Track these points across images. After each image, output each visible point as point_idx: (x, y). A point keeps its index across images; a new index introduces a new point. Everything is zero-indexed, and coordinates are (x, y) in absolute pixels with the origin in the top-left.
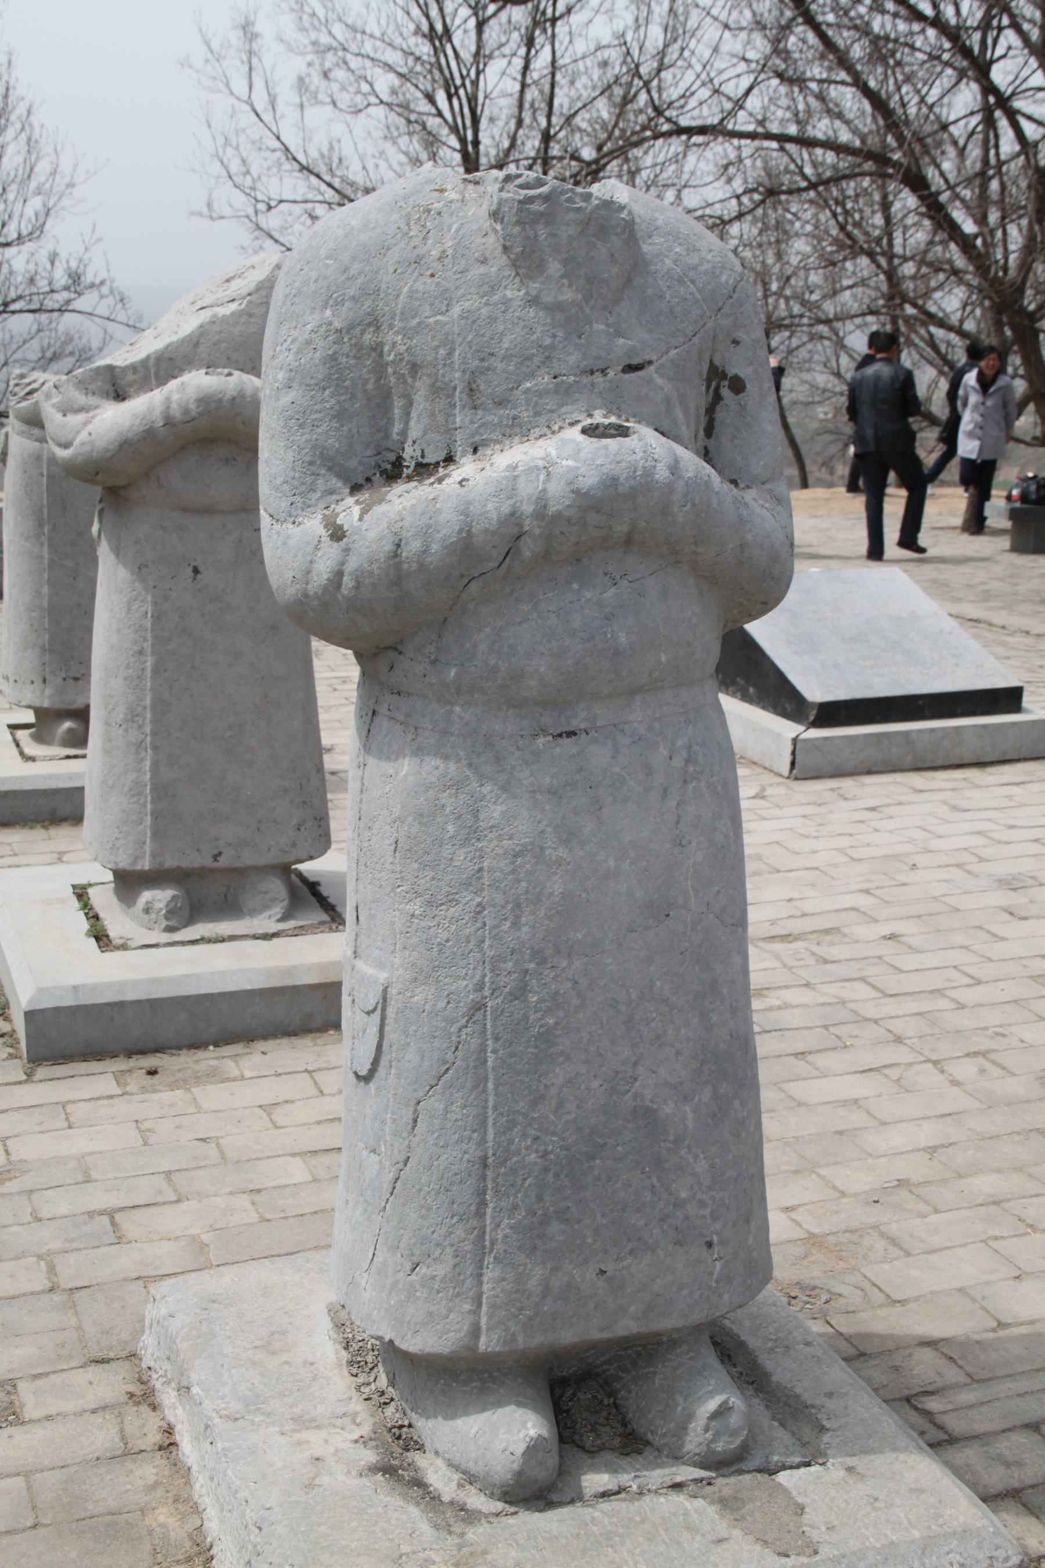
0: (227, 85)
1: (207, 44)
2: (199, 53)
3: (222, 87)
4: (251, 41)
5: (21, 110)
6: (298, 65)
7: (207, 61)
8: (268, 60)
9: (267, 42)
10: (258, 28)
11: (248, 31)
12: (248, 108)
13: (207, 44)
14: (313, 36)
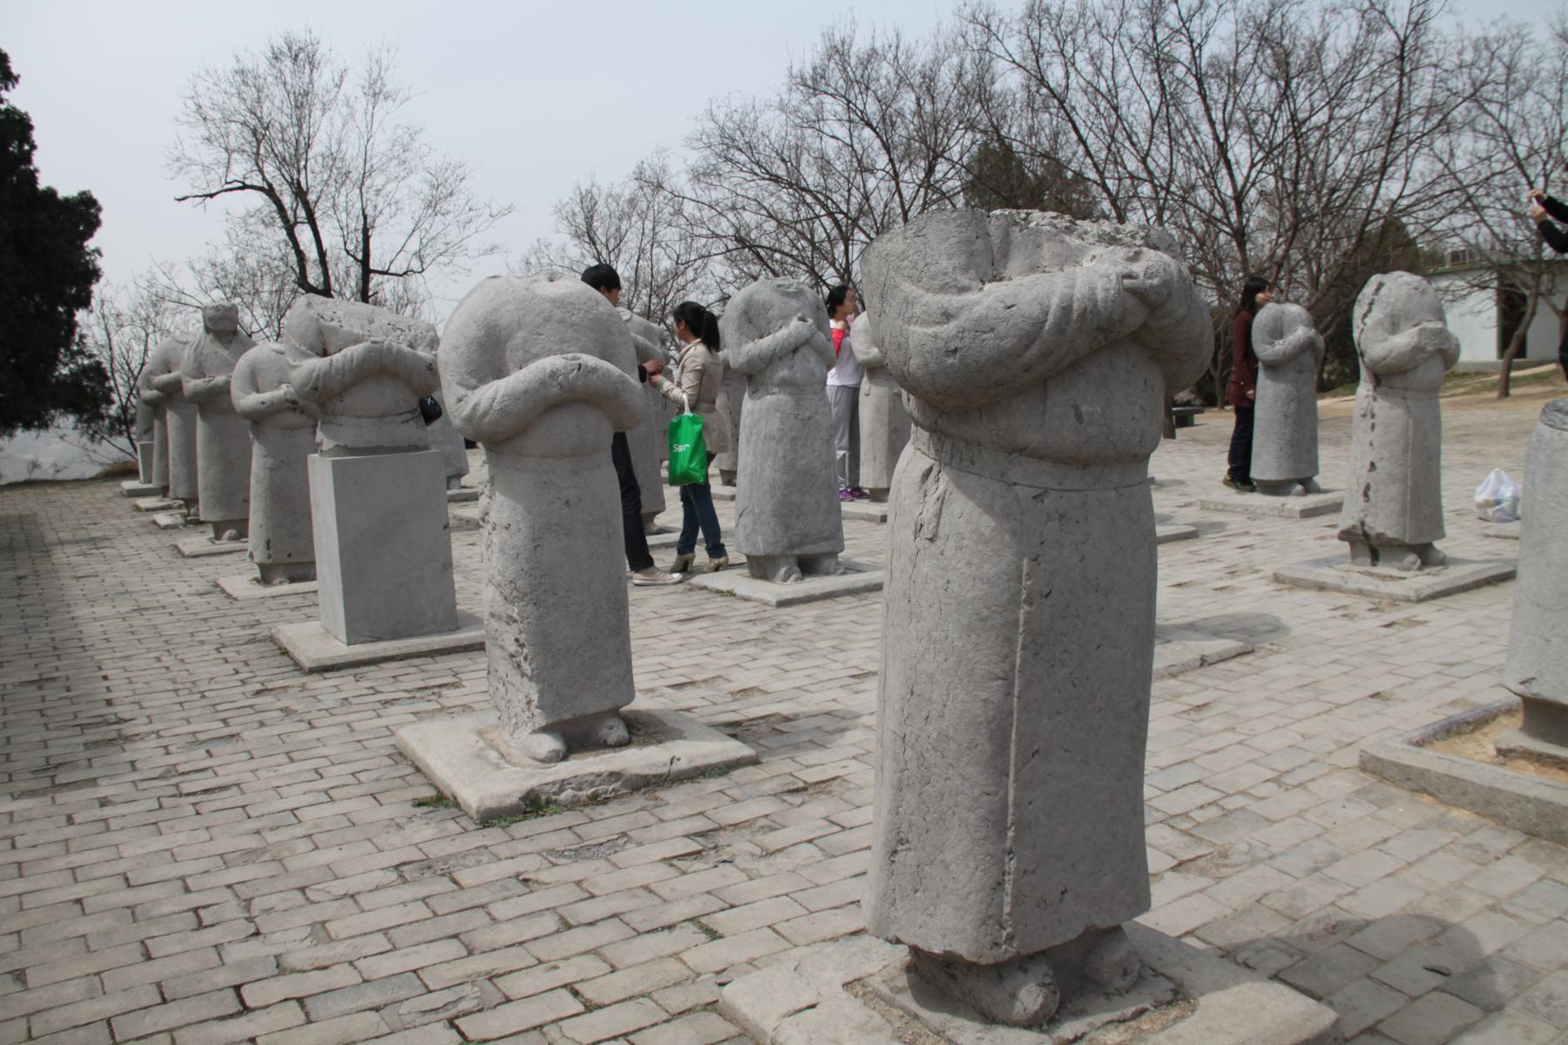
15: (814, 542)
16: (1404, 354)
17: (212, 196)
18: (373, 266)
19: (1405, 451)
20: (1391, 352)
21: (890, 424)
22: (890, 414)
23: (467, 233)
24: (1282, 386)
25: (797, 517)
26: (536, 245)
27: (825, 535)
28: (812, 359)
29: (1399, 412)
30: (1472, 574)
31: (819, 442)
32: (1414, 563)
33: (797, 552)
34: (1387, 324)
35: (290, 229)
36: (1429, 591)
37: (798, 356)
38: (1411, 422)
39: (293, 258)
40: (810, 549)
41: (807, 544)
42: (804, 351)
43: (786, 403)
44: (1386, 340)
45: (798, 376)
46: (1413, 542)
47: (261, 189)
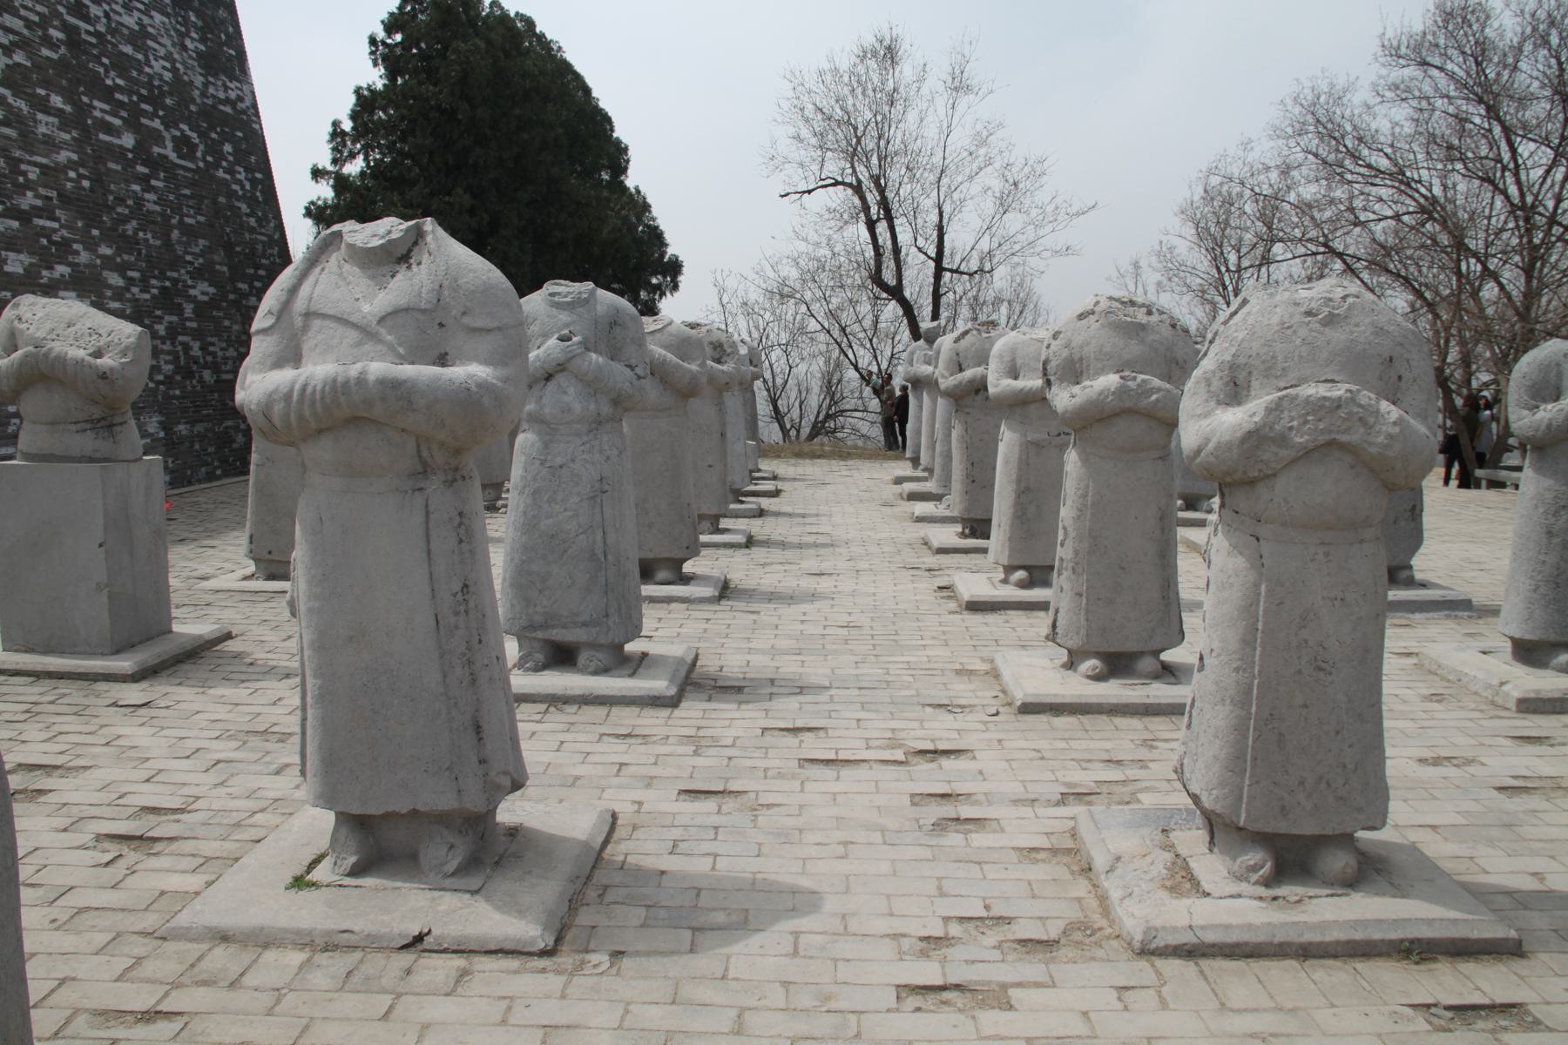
5: (1035, 298)
6: (1158, 276)
8: (1144, 277)
11: (1136, 266)
15: (564, 627)
16: (1228, 446)
17: (809, 192)
18: (945, 265)
19: (1248, 642)
20: (1208, 440)
21: (1019, 481)
22: (1020, 469)
23: (1041, 232)
24: (1549, 482)
25: (541, 591)
27: (581, 619)
28: (571, 390)
29: (1240, 562)
30: (1356, 924)
31: (575, 499)
32: (1254, 869)
33: (540, 634)
34: (1216, 384)
35: (871, 226)
36: (1188, 938)
37: (552, 385)
38: (1263, 588)
39: (870, 253)
40: (559, 635)
41: (553, 627)
42: (560, 379)
43: (532, 445)
44: (1206, 415)
45: (547, 411)
46: (1260, 826)
47: (850, 185)
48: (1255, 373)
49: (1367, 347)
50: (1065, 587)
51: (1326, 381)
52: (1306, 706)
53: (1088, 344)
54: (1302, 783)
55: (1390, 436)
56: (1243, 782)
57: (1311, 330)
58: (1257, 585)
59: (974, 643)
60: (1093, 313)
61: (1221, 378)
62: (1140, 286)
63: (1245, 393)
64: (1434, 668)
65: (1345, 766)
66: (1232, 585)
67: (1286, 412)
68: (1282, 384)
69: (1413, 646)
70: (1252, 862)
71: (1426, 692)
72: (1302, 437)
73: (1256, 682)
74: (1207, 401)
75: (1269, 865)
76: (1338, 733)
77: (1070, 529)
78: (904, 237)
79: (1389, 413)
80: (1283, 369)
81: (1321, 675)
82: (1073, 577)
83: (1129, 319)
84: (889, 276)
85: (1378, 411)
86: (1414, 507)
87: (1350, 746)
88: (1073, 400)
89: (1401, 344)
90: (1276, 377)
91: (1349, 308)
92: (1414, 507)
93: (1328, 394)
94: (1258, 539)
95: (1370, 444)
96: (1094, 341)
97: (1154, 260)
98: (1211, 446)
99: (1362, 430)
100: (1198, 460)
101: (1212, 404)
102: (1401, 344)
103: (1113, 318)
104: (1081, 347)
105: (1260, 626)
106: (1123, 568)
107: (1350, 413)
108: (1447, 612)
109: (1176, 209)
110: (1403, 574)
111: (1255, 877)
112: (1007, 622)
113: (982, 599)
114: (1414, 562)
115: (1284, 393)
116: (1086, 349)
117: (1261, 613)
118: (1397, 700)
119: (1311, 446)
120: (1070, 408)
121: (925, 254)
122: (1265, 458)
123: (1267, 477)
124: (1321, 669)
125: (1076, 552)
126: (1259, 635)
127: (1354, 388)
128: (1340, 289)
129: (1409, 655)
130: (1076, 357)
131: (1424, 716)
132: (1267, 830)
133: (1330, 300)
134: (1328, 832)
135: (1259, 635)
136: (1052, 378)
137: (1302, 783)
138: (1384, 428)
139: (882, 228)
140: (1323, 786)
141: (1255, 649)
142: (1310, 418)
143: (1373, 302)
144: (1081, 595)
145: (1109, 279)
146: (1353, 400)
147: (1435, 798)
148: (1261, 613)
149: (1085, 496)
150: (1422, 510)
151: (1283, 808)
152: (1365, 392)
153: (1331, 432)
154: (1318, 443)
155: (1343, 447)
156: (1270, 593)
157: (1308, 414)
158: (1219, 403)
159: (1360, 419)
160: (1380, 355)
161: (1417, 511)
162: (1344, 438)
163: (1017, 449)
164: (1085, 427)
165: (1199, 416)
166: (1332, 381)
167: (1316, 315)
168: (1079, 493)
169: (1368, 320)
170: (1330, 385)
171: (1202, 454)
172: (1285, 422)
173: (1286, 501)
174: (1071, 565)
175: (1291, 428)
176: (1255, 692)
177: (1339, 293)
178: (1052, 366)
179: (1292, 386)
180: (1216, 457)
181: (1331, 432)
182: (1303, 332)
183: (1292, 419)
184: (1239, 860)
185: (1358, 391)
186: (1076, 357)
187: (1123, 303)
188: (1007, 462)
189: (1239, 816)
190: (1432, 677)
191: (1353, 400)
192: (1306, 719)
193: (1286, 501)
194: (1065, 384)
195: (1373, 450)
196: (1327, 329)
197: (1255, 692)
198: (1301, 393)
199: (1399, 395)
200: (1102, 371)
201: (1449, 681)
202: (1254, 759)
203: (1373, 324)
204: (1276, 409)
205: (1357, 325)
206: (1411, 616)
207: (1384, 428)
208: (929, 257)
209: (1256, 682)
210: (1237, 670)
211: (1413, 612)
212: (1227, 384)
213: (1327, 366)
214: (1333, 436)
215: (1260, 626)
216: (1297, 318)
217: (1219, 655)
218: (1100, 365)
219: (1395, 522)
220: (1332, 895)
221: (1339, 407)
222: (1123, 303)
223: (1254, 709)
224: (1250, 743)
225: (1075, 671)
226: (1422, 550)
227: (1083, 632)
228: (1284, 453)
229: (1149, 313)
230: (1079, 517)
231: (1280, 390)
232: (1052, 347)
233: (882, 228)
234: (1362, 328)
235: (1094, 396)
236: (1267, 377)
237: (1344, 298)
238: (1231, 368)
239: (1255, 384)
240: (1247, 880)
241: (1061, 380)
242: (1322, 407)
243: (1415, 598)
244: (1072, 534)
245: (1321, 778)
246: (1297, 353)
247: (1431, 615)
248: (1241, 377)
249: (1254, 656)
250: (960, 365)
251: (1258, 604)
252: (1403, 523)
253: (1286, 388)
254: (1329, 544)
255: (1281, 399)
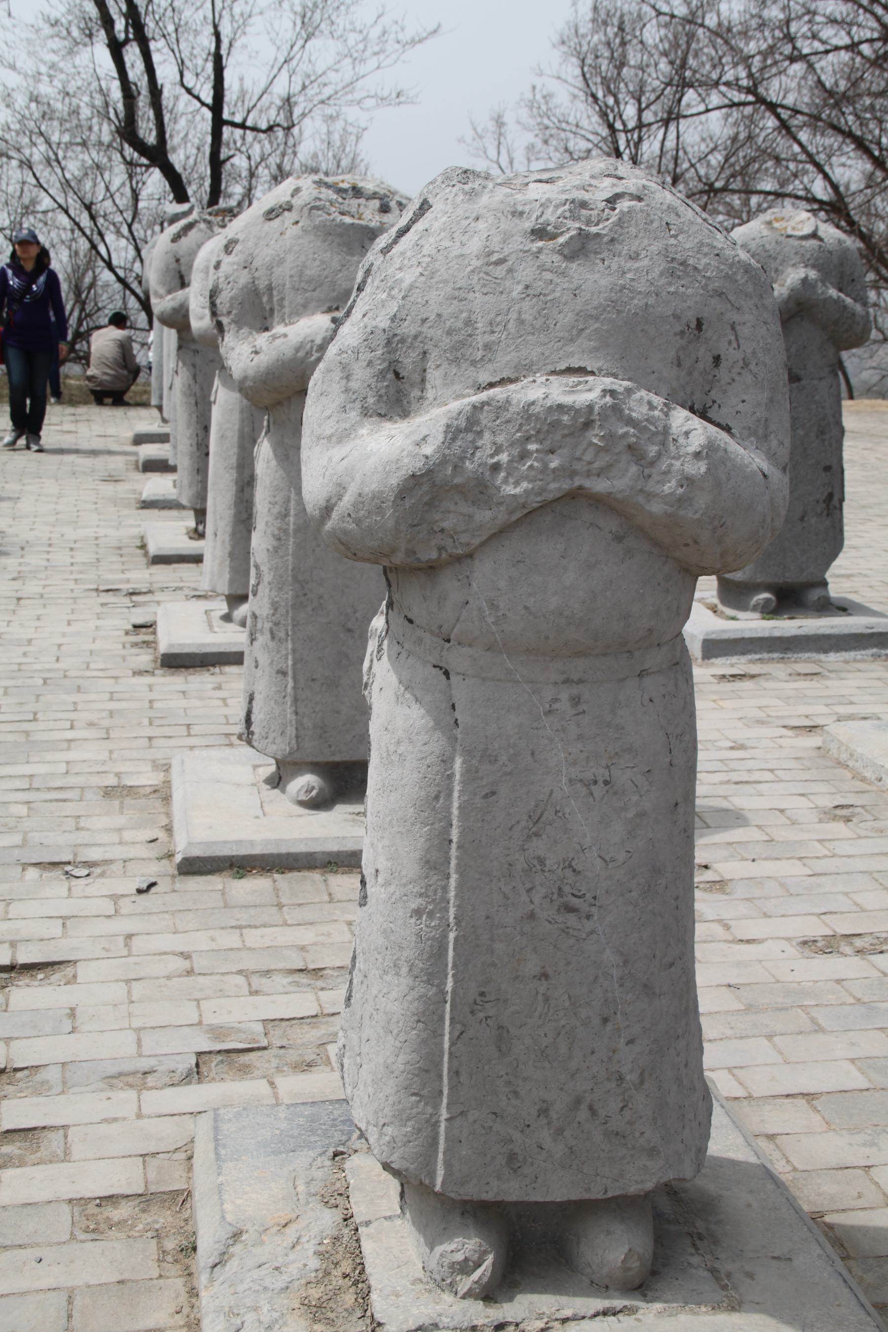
0: (485, 152)
1: (475, 130)
2: (469, 134)
3: (482, 154)
4: (500, 128)
5: (362, 167)
6: (530, 138)
7: (474, 139)
8: (509, 137)
9: (511, 127)
10: (505, 119)
11: (499, 123)
12: (496, 166)
13: (475, 130)
14: (539, 120)
16: (376, 504)
20: (341, 489)
23: (362, 69)
26: (530, 96)
32: (465, 1267)
34: (362, 375)
35: (116, 49)
39: (116, 94)
46: (474, 1191)
48: (434, 354)
49: (651, 300)
50: (261, 662)
51: (569, 371)
52: (545, 976)
53: (281, 262)
54: (544, 1111)
55: (688, 481)
56: (436, 1113)
57: (542, 268)
58: (446, 761)
59: (149, 732)
60: (290, 209)
61: (370, 363)
62: (503, 151)
63: (416, 393)
64: (844, 757)
65: (621, 1079)
66: (402, 758)
67: (487, 435)
68: (485, 377)
69: (819, 712)
70: (459, 1257)
71: (828, 802)
72: (517, 484)
73: (452, 936)
74: (344, 409)
75: (490, 1259)
76: (605, 1020)
77: (264, 568)
78: (166, 73)
79: (687, 434)
80: (487, 347)
81: (572, 920)
82: (271, 644)
83: (348, 220)
84: (148, 133)
85: (666, 430)
86: (831, 496)
87: (630, 1042)
88: (257, 359)
89: (721, 294)
90: (474, 363)
91: (620, 223)
92: (831, 496)
93: (567, 400)
94: (447, 674)
95: (650, 496)
96: (290, 258)
97: (524, 113)
98: (348, 500)
99: (634, 469)
100: (329, 526)
101: (354, 415)
102: (721, 294)
103: (320, 217)
104: (270, 268)
105: (455, 834)
106: (350, 630)
107: (610, 437)
108: (875, 650)
109: (556, 38)
110: (814, 595)
111: (466, 1283)
112: (219, 688)
113: (186, 650)
114: (828, 576)
115: (483, 396)
116: (277, 271)
117: (455, 812)
118: (782, 820)
119: (535, 501)
120: (251, 373)
121: (198, 98)
122: (446, 525)
123: (458, 559)
124: (571, 909)
125: (275, 606)
126: (454, 852)
127: (621, 385)
128: (608, 181)
129: (812, 728)
130: (262, 284)
131: (821, 850)
132: (485, 1197)
133: (584, 205)
134: (596, 1194)
135: (454, 852)
136: (225, 320)
137: (544, 1111)
138: (677, 464)
139: (132, 54)
140: (583, 1114)
141: (448, 877)
142: (532, 447)
143: (671, 209)
144: (284, 674)
145: (461, 140)
146: (616, 409)
147: (819, 1029)
148: (455, 812)
149: (284, 515)
150: (842, 500)
151: (512, 1157)
152: (643, 393)
153: (573, 474)
154: (551, 497)
155: (599, 502)
156: (471, 775)
157: (528, 439)
158: (366, 413)
159: (630, 447)
160: (677, 317)
161: (835, 501)
162: (600, 486)
163: (236, 417)
164: (280, 403)
165: (329, 438)
166: (581, 371)
167: (553, 237)
168: (276, 510)
169: (656, 247)
170: (573, 379)
171: (335, 515)
172: (484, 456)
173: (493, 606)
174: (268, 625)
175: (496, 467)
176: (451, 953)
177: (606, 188)
178: (223, 299)
179: (502, 382)
180: (358, 522)
181: (573, 474)
182: (526, 272)
183: (498, 450)
184: (439, 1249)
185: (629, 391)
186: (262, 284)
187: (340, 191)
188: (222, 437)
189: (432, 1174)
190: (840, 771)
191: (616, 409)
192: (547, 999)
193: (493, 606)
194: (245, 331)
195: (656, 508)
196: (574, 266)
197: (451, 953)
198: (515, 397)
199: (713, 394)
200: (304, 309)
201: (863, 780)
202: (455, 1073)
203: (665, 253)
204: (468, 430)
205: (634, 257)
206: (822, 657)
207: (677, 464)
208: (203, 104)
209: (452, 936)
210: (418, 913)
211: (826, 651)
212: (382, 375)
213: (572, 340)
214: (577, 482)
215: (455, 834)
216: (518, 243)
217: (387, 884)
218: (300, 299)
219: (802, 519)
220: (605, 1313)
221: (588, 425)
222: (340, 191)
223: (450, 985)
224: (446, 1045)
225: (283, 791)
226: (841, 555)
227: (291, 731)
228: (483, 516)
229: (385, 209)
230: (276, 549)
231: (480, 388)
232: (223, 267)
233: (132, 54)
234: (646, 262)
235: (289, 353)
236: (456, 361)
237: (612, 201)
238: (389, 342)
239: (434, 376)
240: (452, 1287)
241: (239, 323)
242: (555, 425)
243: (828, 631)
244: (267, 577)
245: (578, 1101)
246: (513, 316)
247: (852, 654)
248: (408, 361)
249: (445, 889)
250: (182, 277)
251: (449, 795)
252: (813, 521)
253: (491, 385)
254: (581, 681)
255: (477, 408)
